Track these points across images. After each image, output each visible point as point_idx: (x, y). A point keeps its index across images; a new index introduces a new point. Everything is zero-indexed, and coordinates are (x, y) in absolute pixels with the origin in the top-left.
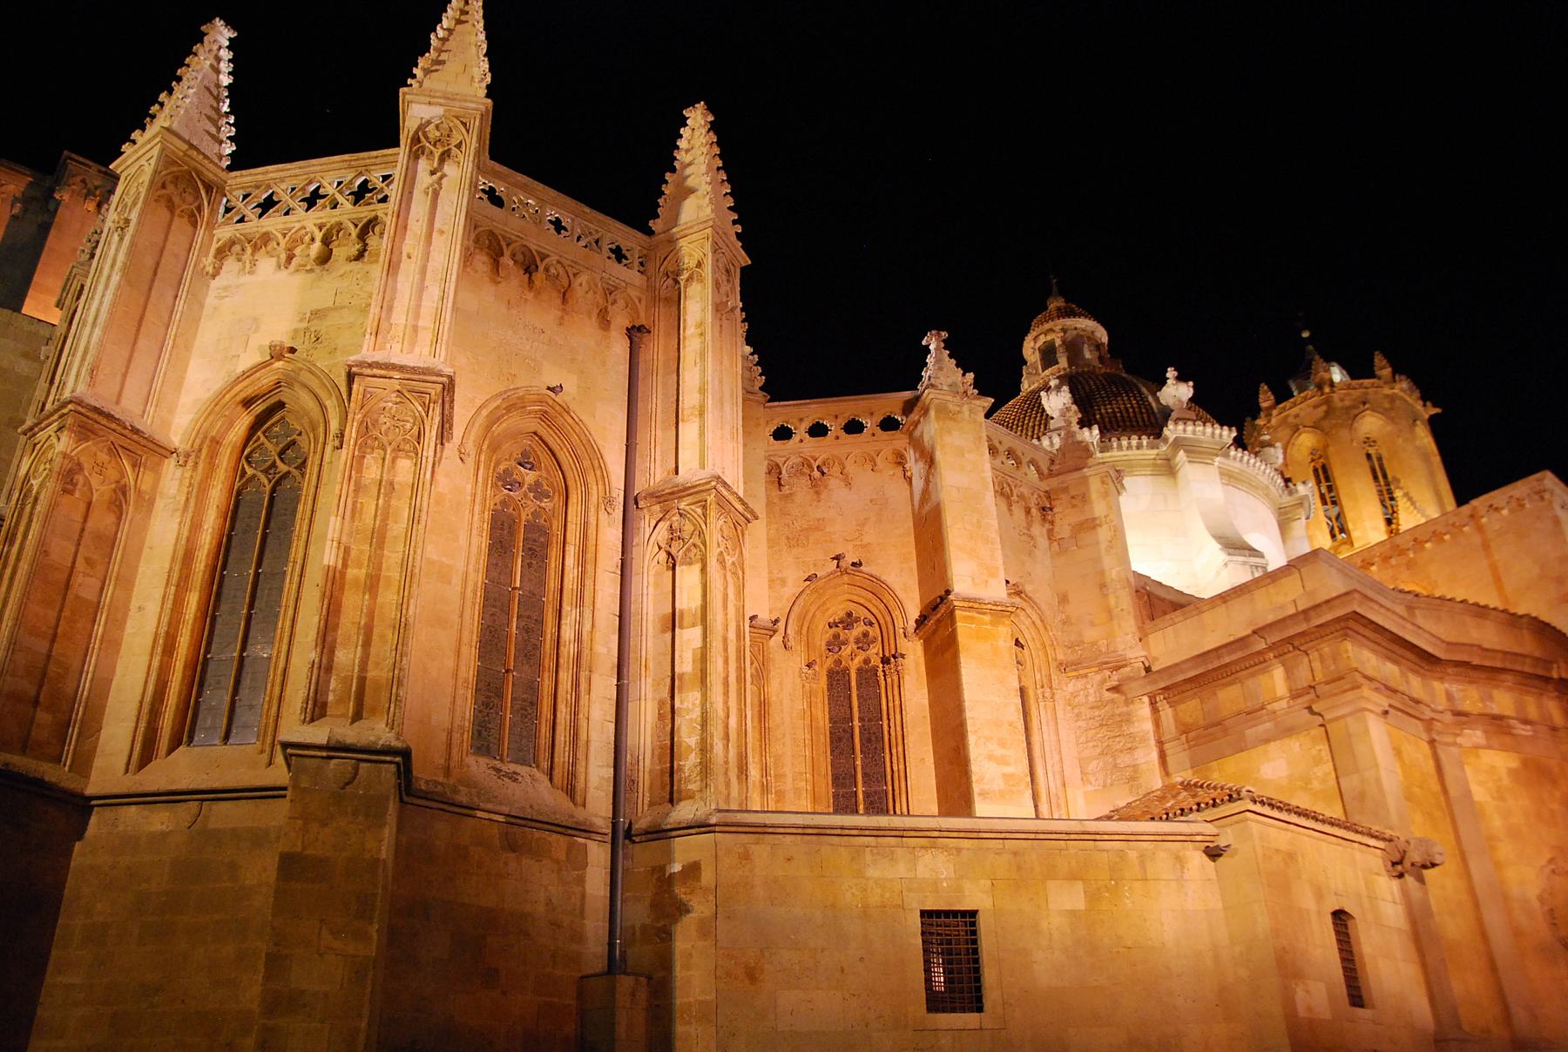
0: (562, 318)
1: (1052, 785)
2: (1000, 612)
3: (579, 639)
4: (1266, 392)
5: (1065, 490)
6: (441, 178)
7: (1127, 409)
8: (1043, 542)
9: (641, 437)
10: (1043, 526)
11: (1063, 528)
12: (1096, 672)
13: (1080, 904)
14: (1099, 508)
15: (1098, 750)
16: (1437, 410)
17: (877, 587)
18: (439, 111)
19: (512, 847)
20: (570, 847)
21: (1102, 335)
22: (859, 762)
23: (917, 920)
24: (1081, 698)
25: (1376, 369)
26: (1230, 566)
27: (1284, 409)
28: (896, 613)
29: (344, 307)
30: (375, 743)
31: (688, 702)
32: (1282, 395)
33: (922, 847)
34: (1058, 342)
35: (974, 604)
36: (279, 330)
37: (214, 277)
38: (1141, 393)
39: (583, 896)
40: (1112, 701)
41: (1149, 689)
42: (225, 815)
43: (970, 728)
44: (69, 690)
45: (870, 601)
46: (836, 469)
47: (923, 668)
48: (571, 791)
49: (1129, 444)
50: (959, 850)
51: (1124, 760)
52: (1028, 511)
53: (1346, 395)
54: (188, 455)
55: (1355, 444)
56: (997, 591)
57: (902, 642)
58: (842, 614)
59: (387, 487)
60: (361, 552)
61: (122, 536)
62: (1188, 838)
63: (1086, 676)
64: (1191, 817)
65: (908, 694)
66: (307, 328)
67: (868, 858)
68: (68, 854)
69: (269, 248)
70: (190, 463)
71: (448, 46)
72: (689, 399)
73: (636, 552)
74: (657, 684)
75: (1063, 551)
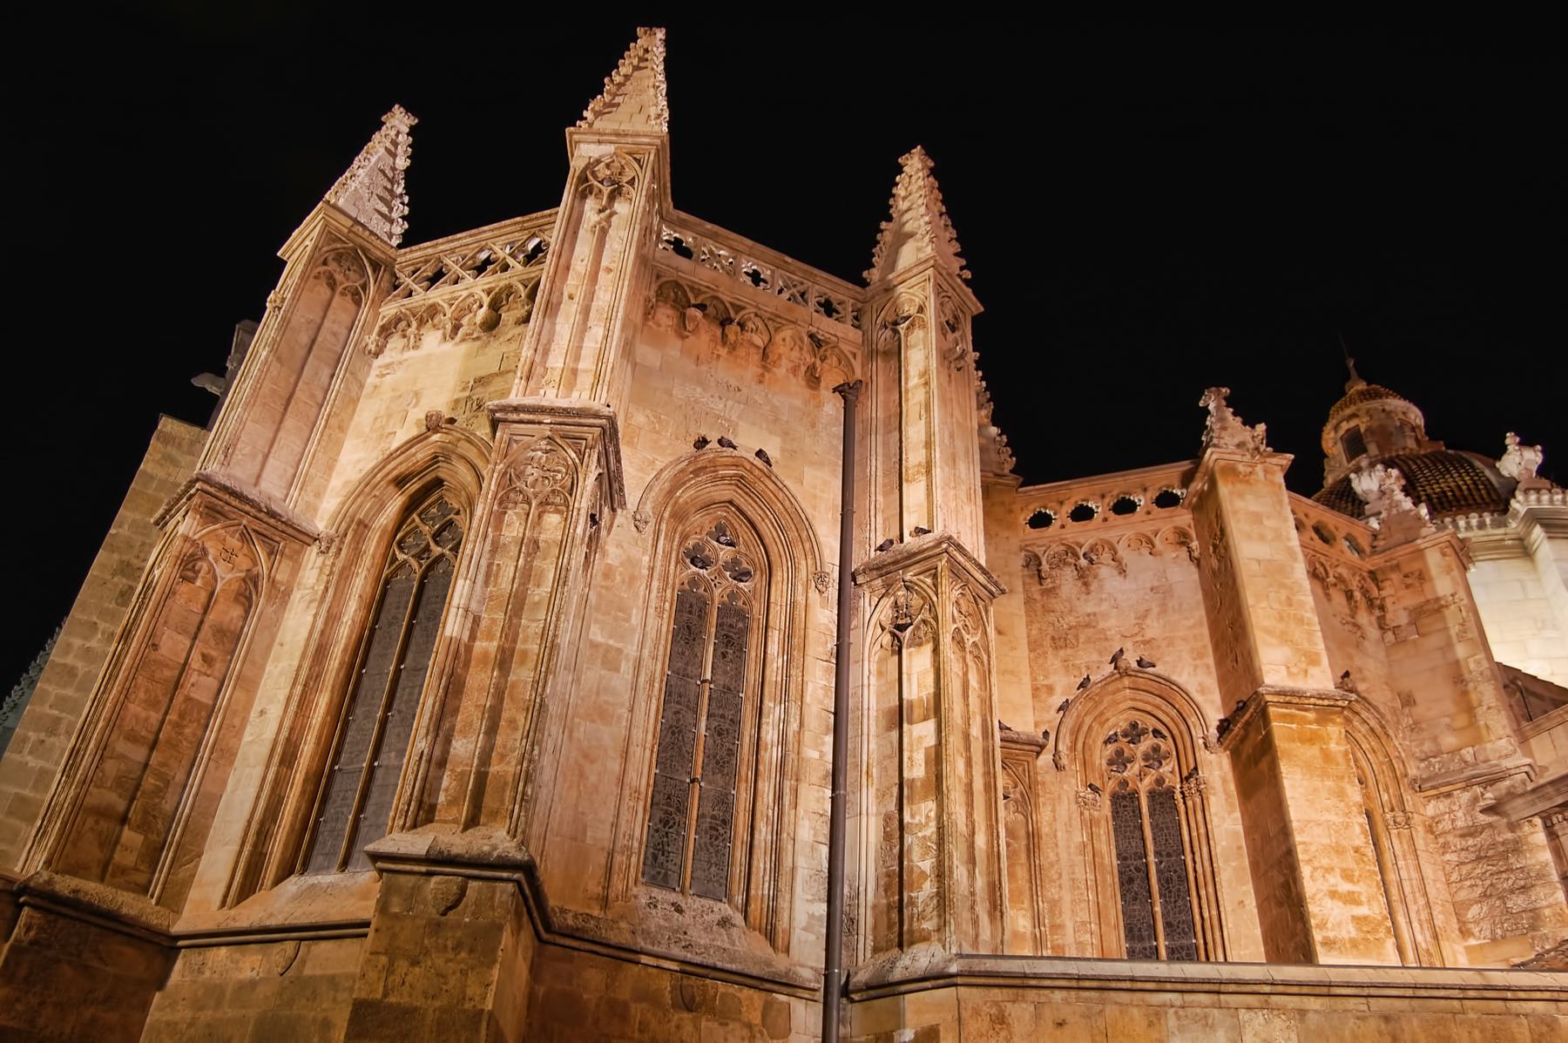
0: (762, 375)
1: (1419, 938)
2: (1325, 708)
5: (1397, 567)
6: (611, 216)
7: (1459, 487)
8: (1373, 632)
10: (1371, 613)
11: (1398, 615)
12: (1464, 789)
15: (1480, 890)
17: (1167, 690)
18: (611, 148)
19: (688, 1004)
20: (767, 1007)
21: (1416, 416)
22: (1158, 909)
24: (1446, 825)
28: (1192, 720)
30: (490, 854)
31: (922, 813)
33: (1249, 1008)
35: (1292, 698)
36: (439, 400)
37: (377, 355)
38: (1472, 466)
40: (1490, 825)
41: (1543, 806)
43: (1301, 856)
44: (168, 807)
45: (1158, 707)
47: (1232, 787)
48: (770, 935)
49: (1468, 523)
50: (1302, 1013)
51: (1517, 902)
52: (1349, 595)
56: (1321, 680)
57: (1203, 755)
58: (1124, 725)
59: (533, 547)
60: (493, 621)
61: (248, 630)
63: (1448, 795)
65: (1215, 820)
66: (469, 397)
67: (1172, 1022)
68: (145, 1007)
69: (436, 321)
70: (333, 550)
72: (914, 457)
73: (854, 637)
74: (882, 796)
75: (1400, 642)
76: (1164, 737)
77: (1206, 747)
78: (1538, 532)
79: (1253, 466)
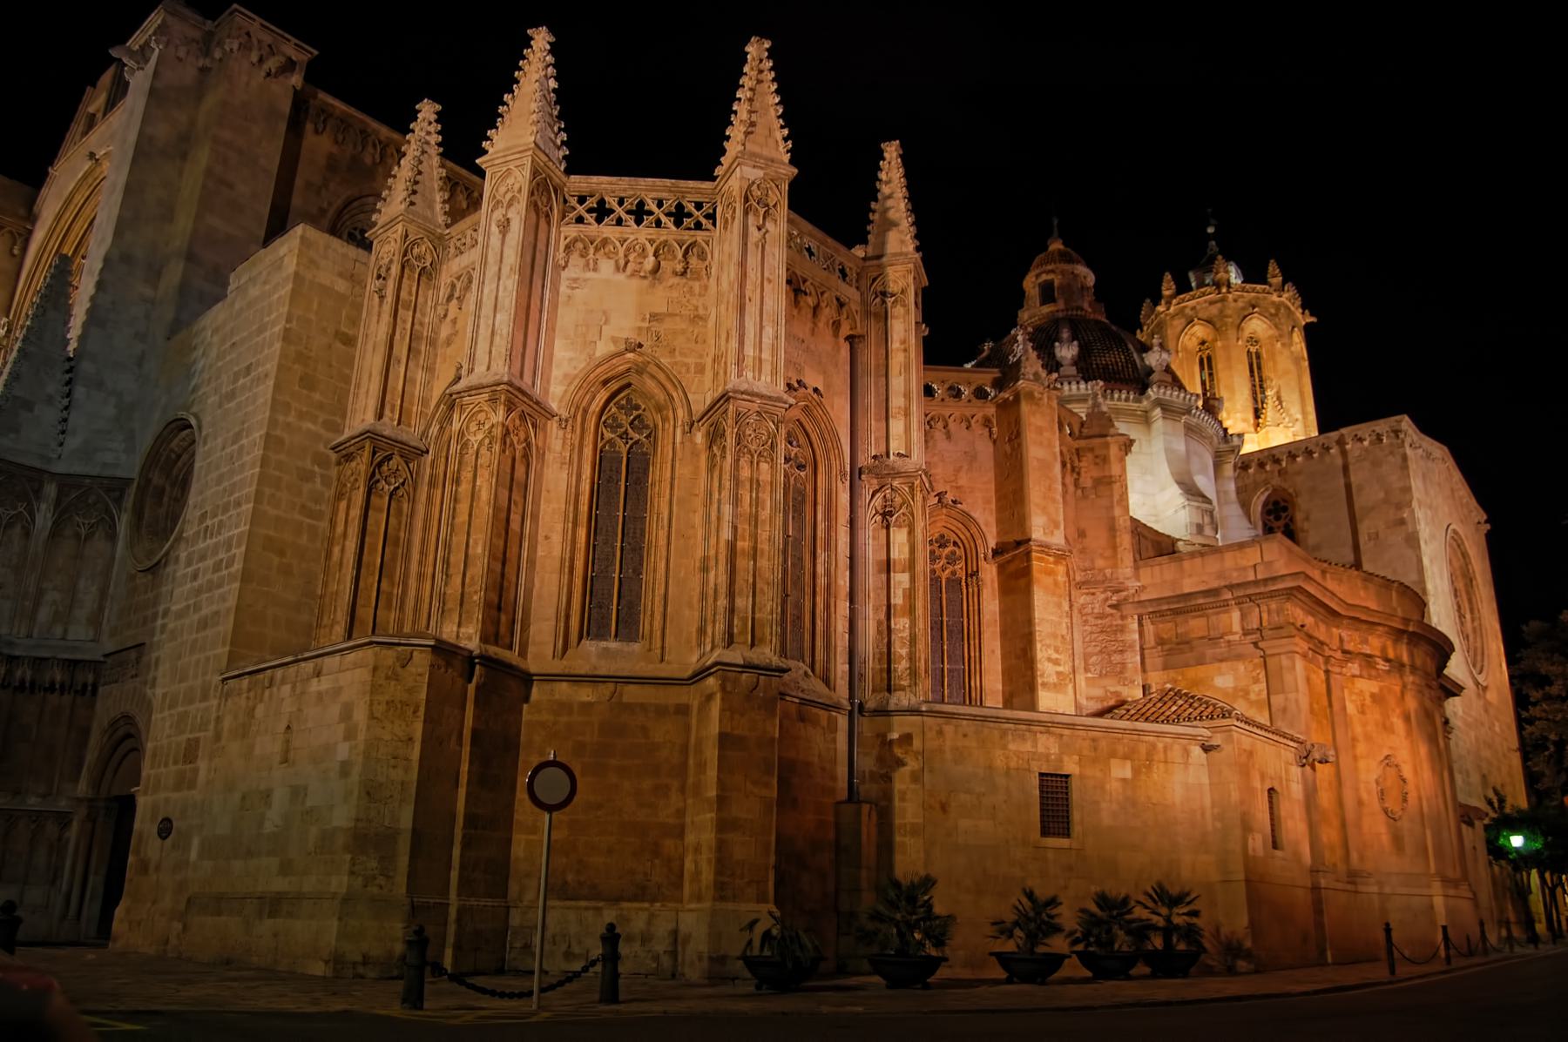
2: (1060, 557)
3: (828, 573)
4: (1169, 282)
5: (1092, 450)
6: (765, 234)
7: (1116, 362)
8: (1071, 488)
9: (860, 422)
10: (1072, 475)
11: (1086, 481)
12: (1102, 593)
13: (1128, 774)
14: (1115, 470)
15: (1099, 648)
16: (1313, 319)
17: (967, 519)
18: (760, 173)
19: (802, 719)
20: (830, 717)
21: (1091, 279)
23: (1036, 781)
24: (1088, 610)
25: (1269, 276)
26: (1187, 508)
27: (1183, 300)
28: (979, 542)
29: (676, 315)
32: (1183, 287)
33: (1041, 733)
34: (1056, 283)
35: (1044, 548)
36: (624, 326)
37: (564, 268)
38: (1128, 350)
39: (836, 749)
40: (1112, 615)
41: (1140, 611)
42: (632, 693)
45: (960, 530)
46: (940, 425)
47: (996, 585)
48: (827, 681)
49: (1120, 397)
50: (1062, 735)
51: (1116, 658)
54: (567, 421)
55: (1240, 342)
56: (1058, 539)
57: (982, 563)
60: (744, 529)
62: (1193, 738)
63: (1093, 594)
64: (1195, 723)
66: (648, 329)
67: (1010, 737)
69: (607, 250)
70: (569, 428)
71: (756, 105)
72: (897, 401)
73: (860, 512)
74: (876, 609)
75: (1085, 497)
76: (959, 547)
77: (985, 559)
78: (1158, 412)
79: (1042, 394)
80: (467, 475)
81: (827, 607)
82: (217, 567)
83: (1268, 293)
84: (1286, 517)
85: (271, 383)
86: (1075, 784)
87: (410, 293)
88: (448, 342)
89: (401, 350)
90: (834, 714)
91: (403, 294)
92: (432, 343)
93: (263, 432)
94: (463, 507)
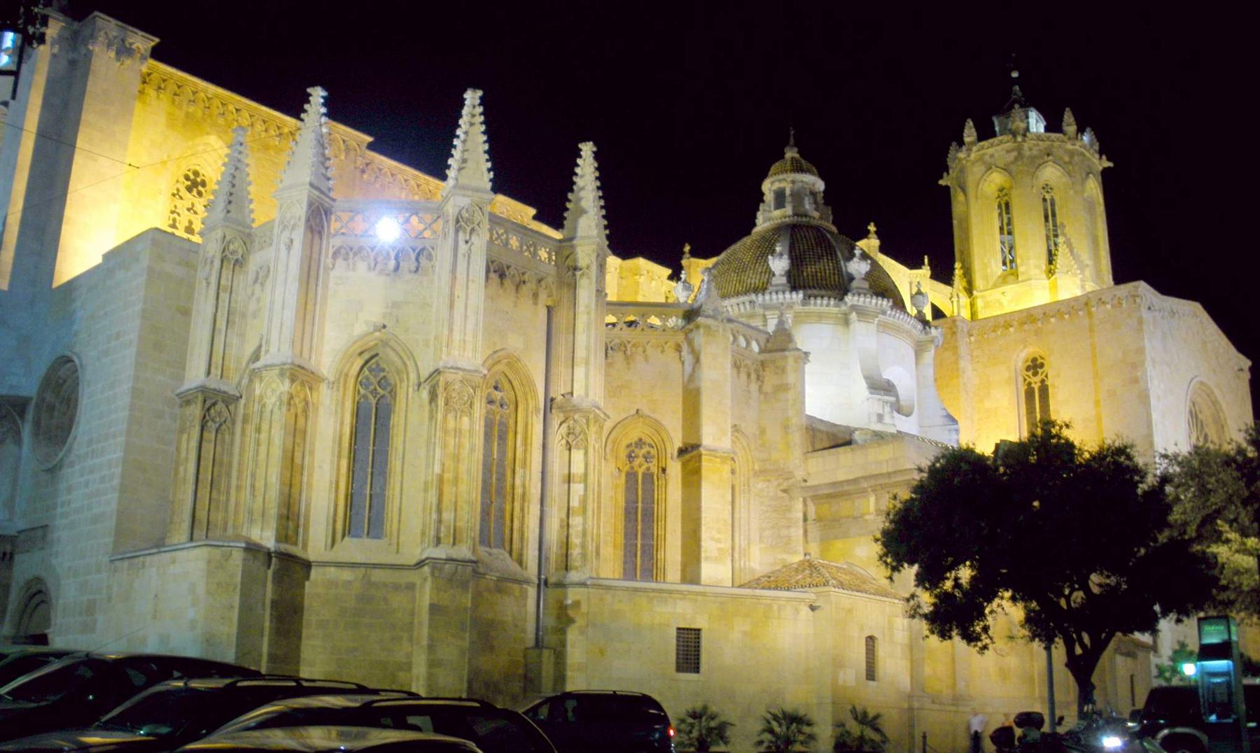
3: (524, 486)
4: (970, 128)
8: (755, 394)
9: (553, 371)
11: (768, 388)
14: (791, 378)
15: (770, 525)
16: (1111, 164)
17: (658, 427)
20: (521, 590)
21: (820, 185)
22: (639, 527)
23: (674, 633)
25: (1064, 124)
26: (871, 400)
27: (982, 148)
31: (576, 521)
32: (985, 133)
34: (788, 192)
35: (712, 451)
36: (374, 313)
37: (332, 269)
42: (378, 575)
43: (703, 522)
44: (296, 511)
46: (641, 349)
48: (520, 562)
51: (784, 532)
52: (749, 375)
53: (1035, 145)
54: (333, 383)
55: (1034, 191)
57: (669, 461)
58: (636, 439)
59: (458, 432)
61: (309, 429)
62: (803, 600)
63: (769, 481)
64: (806, 589)
68: (303, 587)
69: (362, 254)
71: (469, 144)
72: (580, 353)
76: (653, 447)
77: (672, 458)
78: (854, 316)
79: (718, 327)
80: (265, 427)
81: (522, 510)
82: (103, 480)
83: (1063, 141)
84: (1042, 373)
85: (134, 350)
86: (704, 635)
87: (227, 280)
88: (255, 316)
89: (221, 324)
90: (525, 586)
91: (223, 282)
92: (244, 315)
93: (130, 385)
94: (263, 449)
